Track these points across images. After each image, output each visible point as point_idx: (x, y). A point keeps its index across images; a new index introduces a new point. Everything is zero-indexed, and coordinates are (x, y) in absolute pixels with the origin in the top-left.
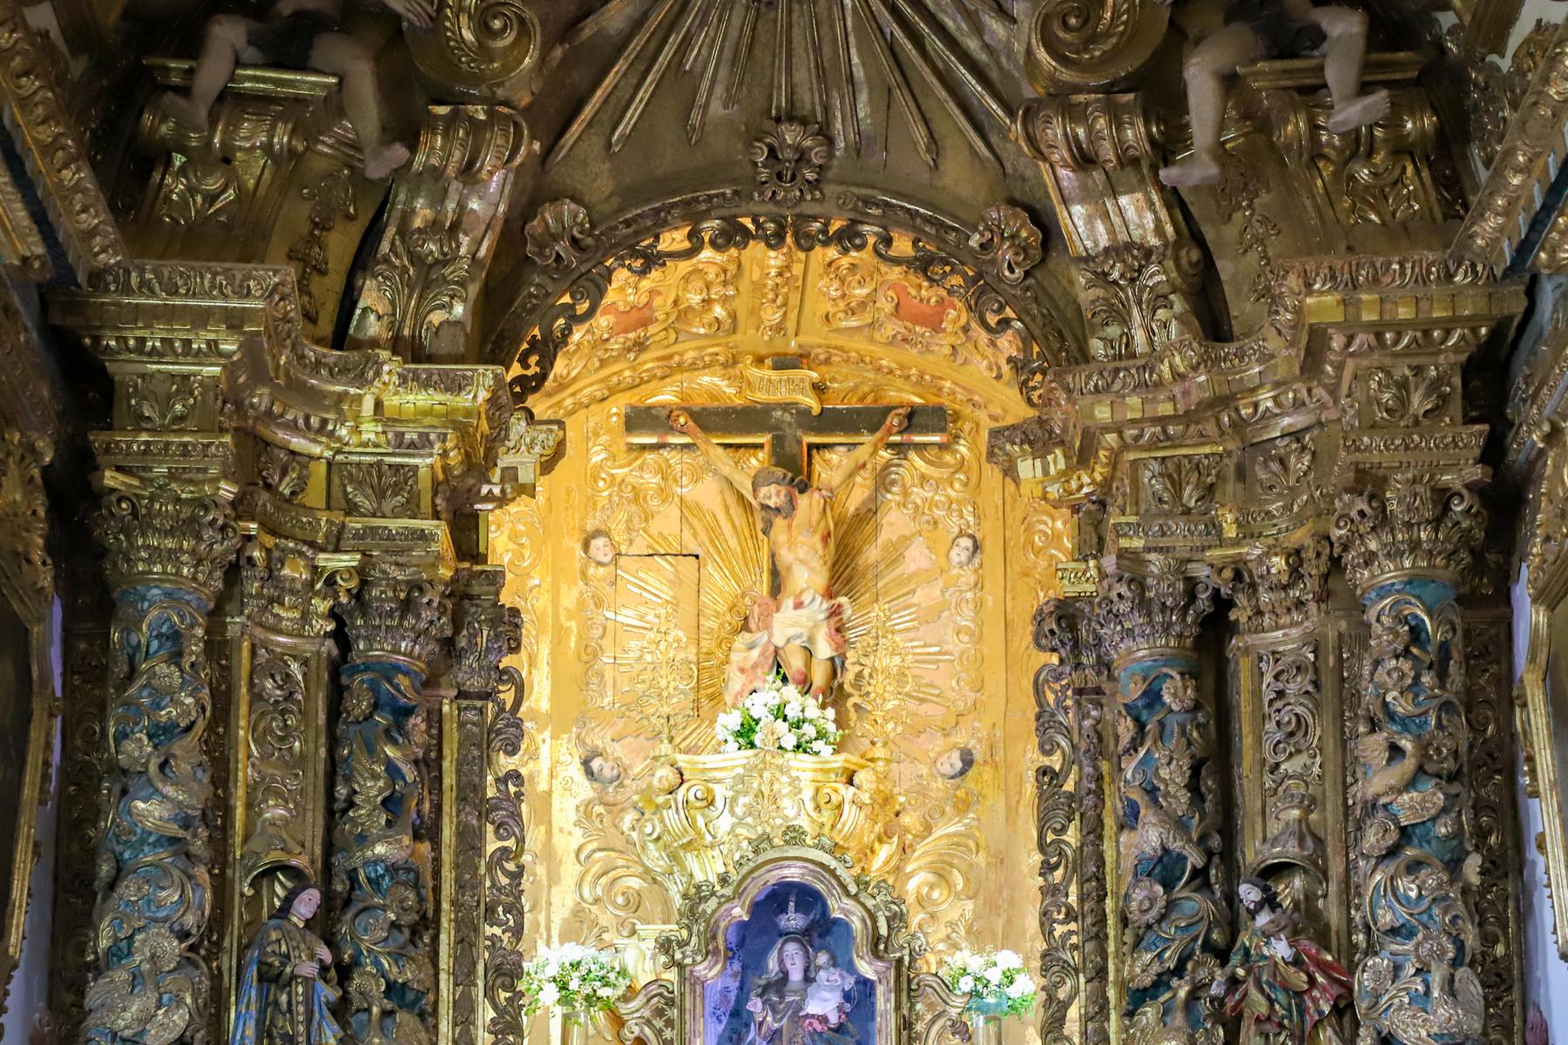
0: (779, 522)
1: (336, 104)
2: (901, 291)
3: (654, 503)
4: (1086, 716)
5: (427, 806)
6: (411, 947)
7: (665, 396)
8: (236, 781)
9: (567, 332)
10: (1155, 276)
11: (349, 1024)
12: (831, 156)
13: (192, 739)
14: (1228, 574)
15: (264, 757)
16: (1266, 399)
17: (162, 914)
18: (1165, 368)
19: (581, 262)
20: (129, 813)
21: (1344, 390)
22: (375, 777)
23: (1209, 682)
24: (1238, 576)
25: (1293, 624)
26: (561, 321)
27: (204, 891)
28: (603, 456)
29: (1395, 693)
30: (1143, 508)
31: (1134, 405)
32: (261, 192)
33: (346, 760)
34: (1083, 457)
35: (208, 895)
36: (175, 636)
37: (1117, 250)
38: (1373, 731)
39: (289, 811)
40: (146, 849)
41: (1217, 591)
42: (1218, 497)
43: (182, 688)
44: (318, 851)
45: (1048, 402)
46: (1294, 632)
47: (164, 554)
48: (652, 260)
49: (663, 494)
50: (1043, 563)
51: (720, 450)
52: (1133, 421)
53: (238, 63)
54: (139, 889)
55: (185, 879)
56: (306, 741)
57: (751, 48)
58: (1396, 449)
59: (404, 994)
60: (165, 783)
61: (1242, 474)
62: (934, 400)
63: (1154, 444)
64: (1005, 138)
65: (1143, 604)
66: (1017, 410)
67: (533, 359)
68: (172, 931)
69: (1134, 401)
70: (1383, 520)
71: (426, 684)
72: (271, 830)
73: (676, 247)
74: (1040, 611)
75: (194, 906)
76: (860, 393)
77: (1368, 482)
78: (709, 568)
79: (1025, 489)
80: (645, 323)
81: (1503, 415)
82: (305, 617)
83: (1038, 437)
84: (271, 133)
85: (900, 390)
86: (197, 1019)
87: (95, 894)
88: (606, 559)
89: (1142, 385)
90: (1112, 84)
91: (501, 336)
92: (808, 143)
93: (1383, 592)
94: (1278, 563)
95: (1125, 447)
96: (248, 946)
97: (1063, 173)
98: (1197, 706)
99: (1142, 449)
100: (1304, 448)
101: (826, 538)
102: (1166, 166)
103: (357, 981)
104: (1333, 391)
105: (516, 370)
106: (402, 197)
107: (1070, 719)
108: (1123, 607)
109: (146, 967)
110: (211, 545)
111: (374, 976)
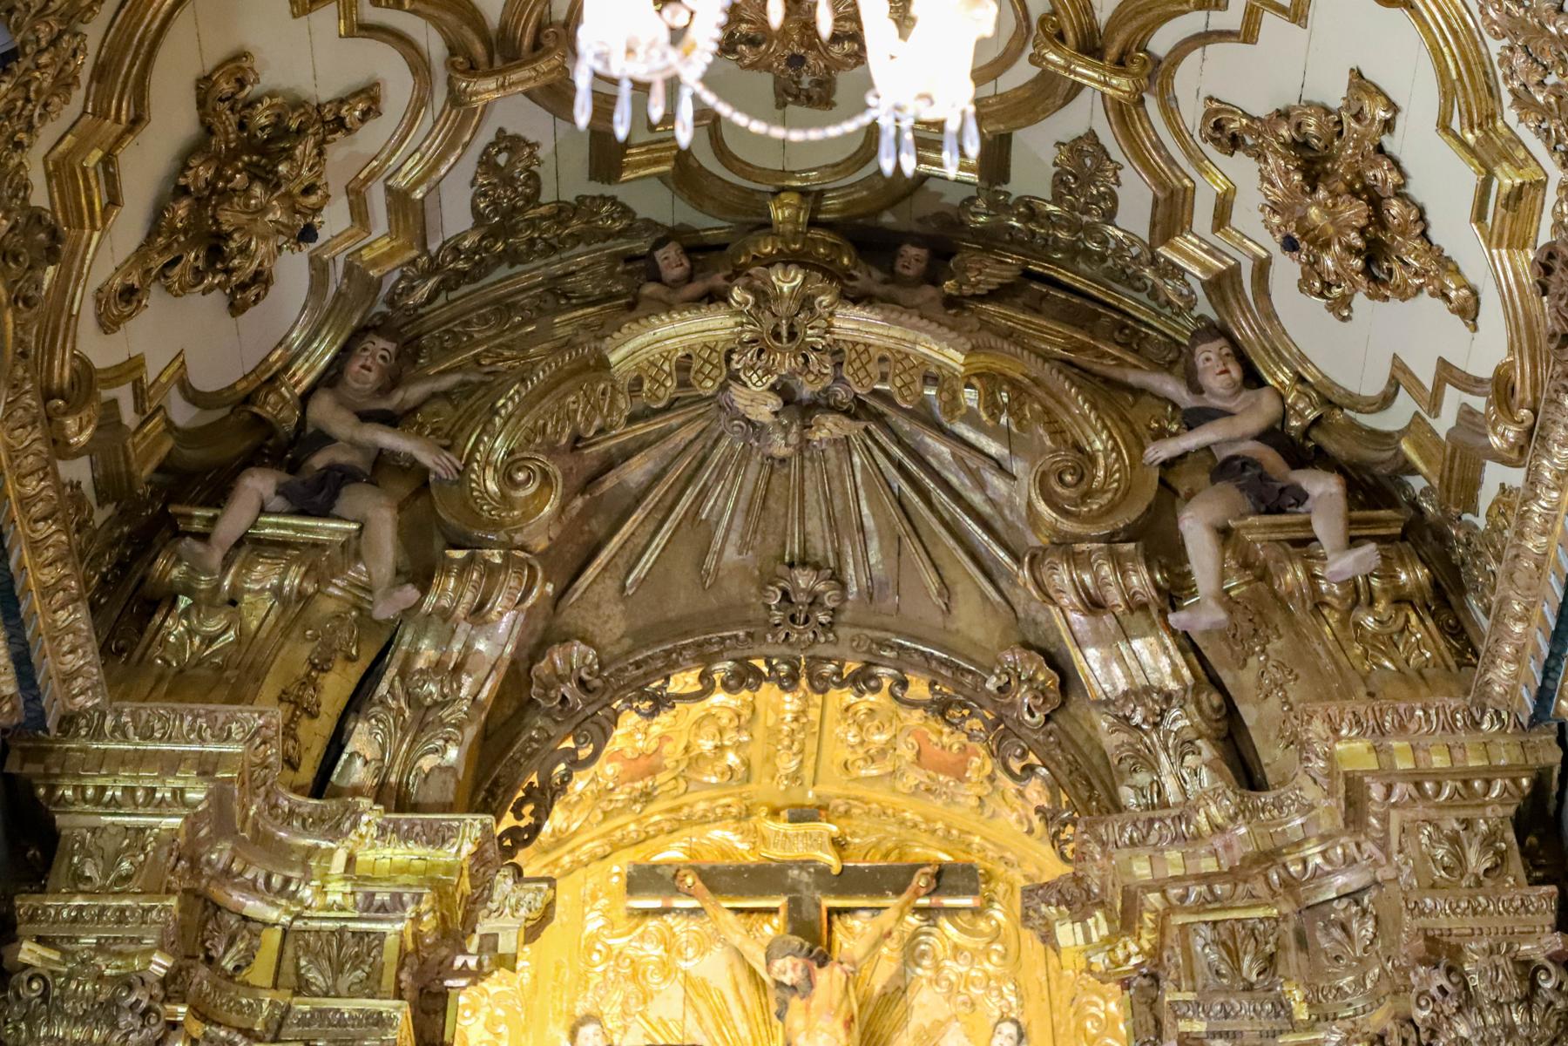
2: (922, 738)
3: (654, 980)
7: (672, 852)
9: (567, 778)
12: (844, 599)
18: (1201, 818)
19: (587, 704)
21: (1394, 846)
26: (562, 767)
28: (601, 922)
45: (1081, 857)
48: (661, 702)
51: (730, 916)
52: (1176, 879)
57: (765, 499)
58: (1463, 913)
63: (1201, 906)
67: (528, 809)
69: (1174, 855)
73: (688, 690)
76: (883, 849)
80: (652, 772)
85: (925, 846)
89: (1179, 838)
91: (496, 783)
92: (821, 587)
95: (1170, 909)
100: (1364, 912)
104: (1383, 846)
105: (509, 820)
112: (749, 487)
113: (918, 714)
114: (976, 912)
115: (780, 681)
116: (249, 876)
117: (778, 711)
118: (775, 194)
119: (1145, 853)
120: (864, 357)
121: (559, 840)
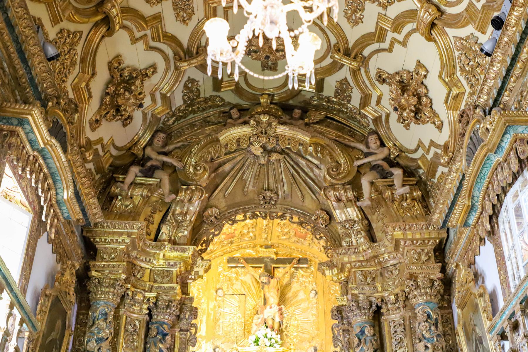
0: (266, 286)
1: (159, 186)
4: (345, 337)
10: (357, 227)
12: (278, 198)
14: (380, 300)
16: (386, 256)
19: (217, 222)
23: (377, 328)
24: (382, 301)
25: (398, 313)
26: (211, 236)
29: (425, 332)
30: (357, 283)
31: (354, 258)
32: (139, 205)
34: (342, 270)
37: (347, 221)
38: (420, 342)
41: (377, 306)
42: (376, 280)
46: (398, 315)
48: (234, 222)
49: (237, 279)
50: (333, 298)
51: (251, 268)
53: (136, 176)
57: (259, 174)
61: (381, 275)
62: (305, 256)
63: (359, 267)
64: (320, 195)
65: (359, 307)
66: (324, 258)
67: (204, 245)
70: (418, 287)
73: (241, 219)
74: (332, 309)
77: (413, 277)
78: (248, 298)
79: (327, 278)
80: (233, 237)
81: (444, 262)
83: (331, 265)
84: (143, 192)
88: (222, 295)
90: (345, 183)
92: (273, 195)
93: (419, 305)
94: (392, 297)
95: (352, 268)
97: (334, 203)
98: (374, 335)
99: (356, 268)
100: (396, 269)
101: (278, 290)
102: (358, 201)
104: (402, 255)
106: (173, 206)
107: (341, 338)
108: (354, 308)
112: (255, 171)
113: (296, 225)
114: (307, 268)
115: (262, 217)
116: (141, 258)
117: (262, 224)
118: (261, 95)
119: (347, 256)
120: (284, 139)
121: (212, 252)
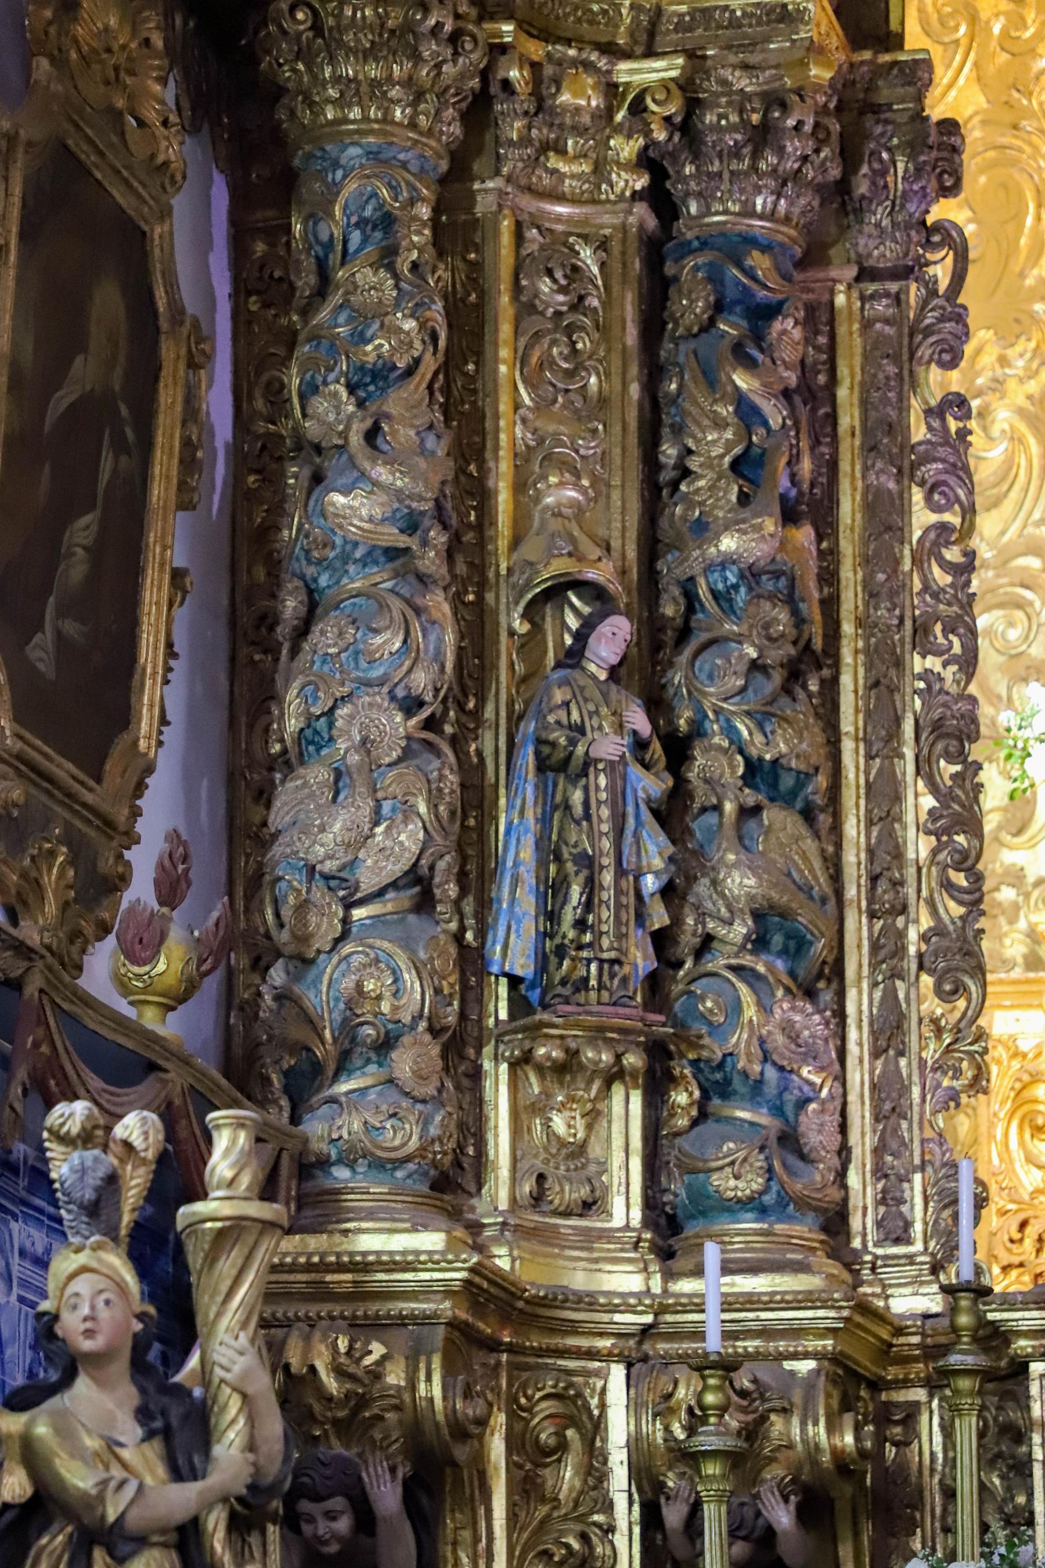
5: (806, 465)
6: (784, 700)
8: (497, 448)
11: (691, 833)
13: (416, 388)
15: (542, 406)
17: (377, 673)
20: (323, 515)
22: (720, 424)
27: (443, 629)
33: (674, 400)
35: (450, 638)
36: (387, 221)
39: (583, 491)
40: (352, 569)
43: (397, 304)
44: (632, 554)
47: (364, 88)
54: (341, 634)
55: (410, 613)
56: (608, 375)
59: (776, 778)
60: (374, 461)
68: (393, 698)
71: (801, 264)
72: (555, 525)
75: (426, 657)
82: (600, 170)
86: (438, 839)
87: (280, 644)
96: (521, 717)
103: (700, 761)
109: (354, 759)
110: (438, 66)
111: (725, 751)
